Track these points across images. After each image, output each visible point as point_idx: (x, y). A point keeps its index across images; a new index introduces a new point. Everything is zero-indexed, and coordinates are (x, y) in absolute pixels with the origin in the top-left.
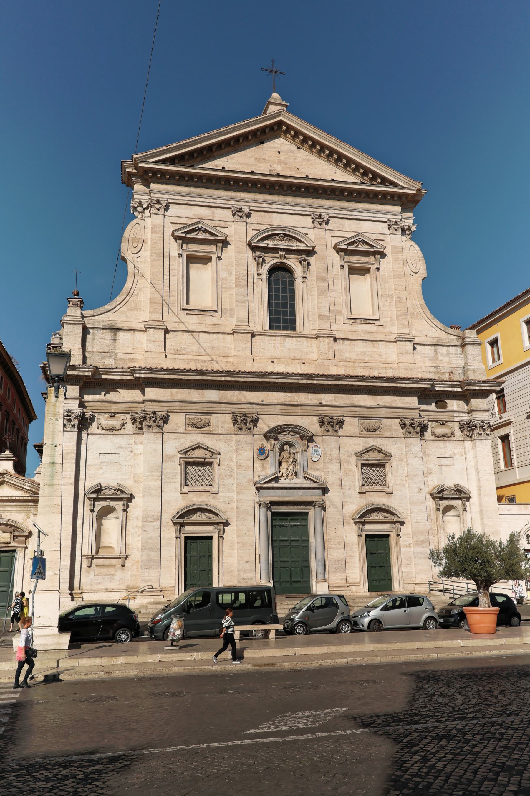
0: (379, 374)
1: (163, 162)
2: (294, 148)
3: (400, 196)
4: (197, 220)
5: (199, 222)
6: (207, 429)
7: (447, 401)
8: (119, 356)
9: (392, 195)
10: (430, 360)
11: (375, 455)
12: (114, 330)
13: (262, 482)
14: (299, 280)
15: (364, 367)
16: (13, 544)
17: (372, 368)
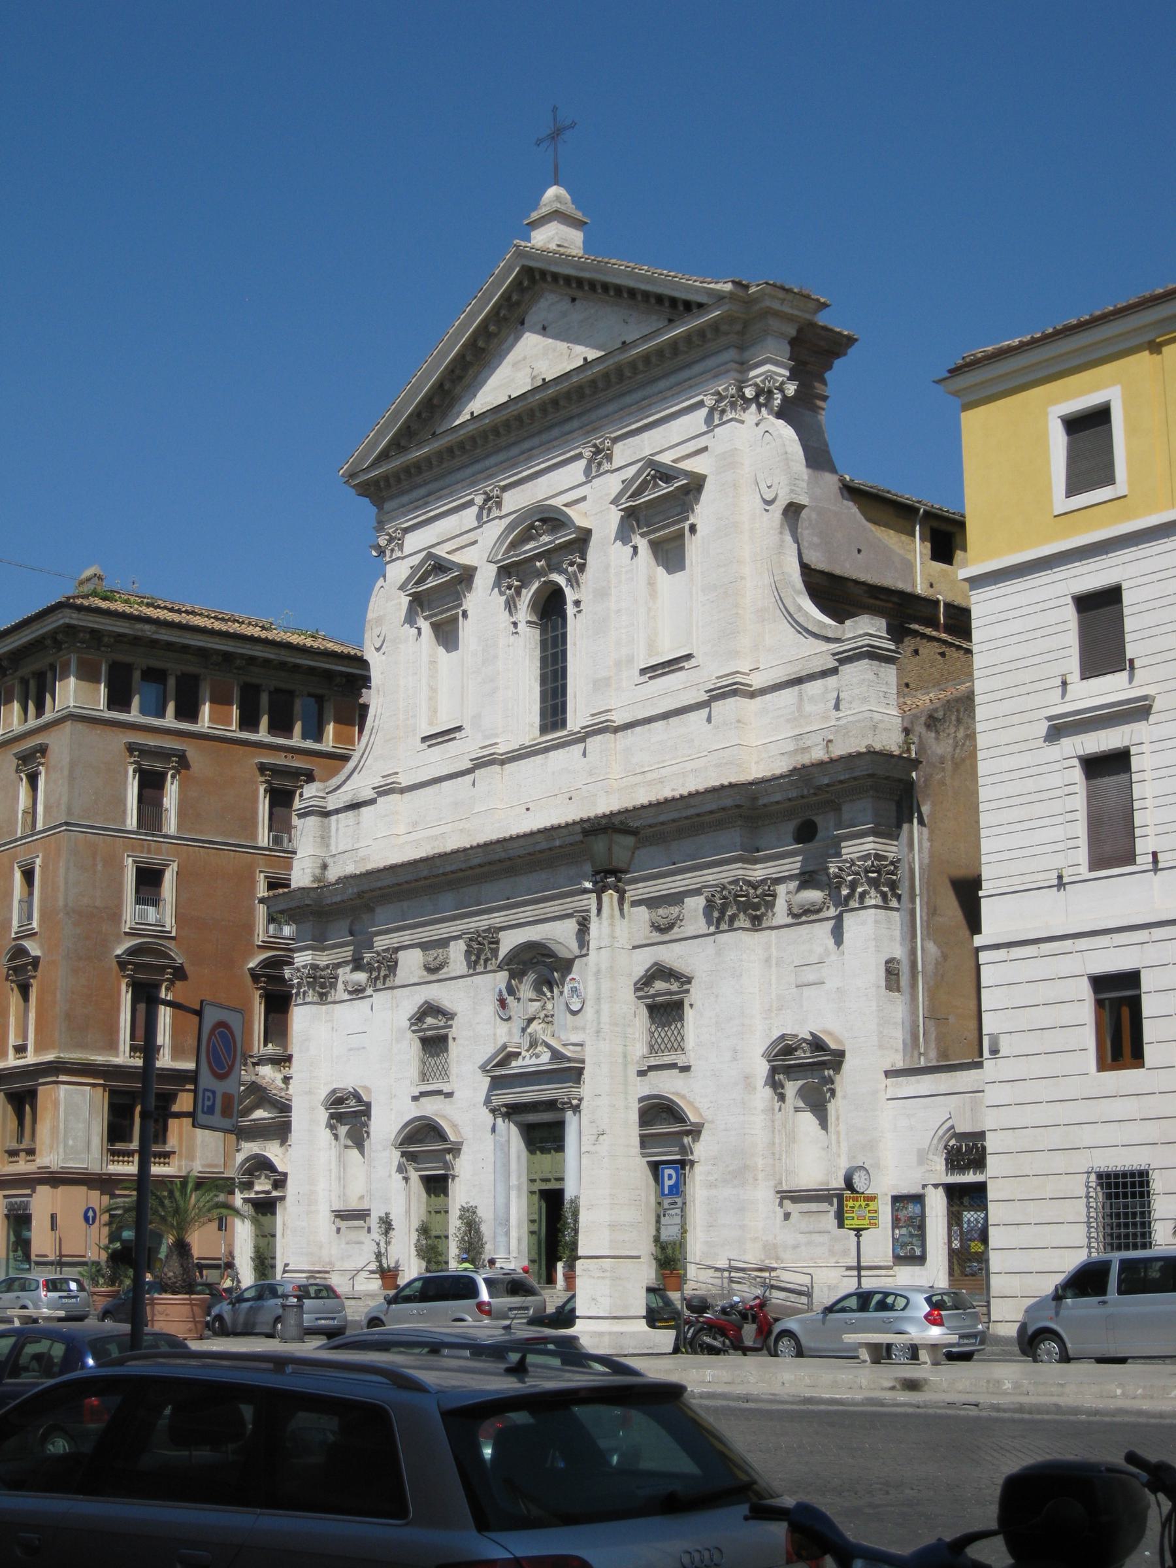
0: (673, 790)
1: (384, 456)
2: (565, 305)
3: (715, 327)
4: (424, 553)
5: (430, 556)
6: (445, 970)
7: (819, 820)
8: (361, 853)
9: (701, 333)
10: (788, 721)
11: (659, 985)
12: (355, 806)
13: (488, 1068)
14: (570, 610)
15: (650, 783)
16: (275, 1194)
17: (661, 781)
